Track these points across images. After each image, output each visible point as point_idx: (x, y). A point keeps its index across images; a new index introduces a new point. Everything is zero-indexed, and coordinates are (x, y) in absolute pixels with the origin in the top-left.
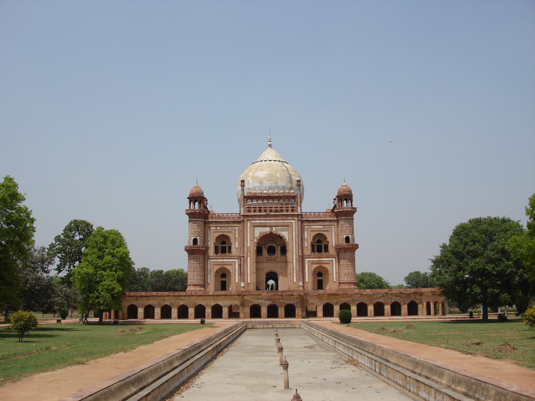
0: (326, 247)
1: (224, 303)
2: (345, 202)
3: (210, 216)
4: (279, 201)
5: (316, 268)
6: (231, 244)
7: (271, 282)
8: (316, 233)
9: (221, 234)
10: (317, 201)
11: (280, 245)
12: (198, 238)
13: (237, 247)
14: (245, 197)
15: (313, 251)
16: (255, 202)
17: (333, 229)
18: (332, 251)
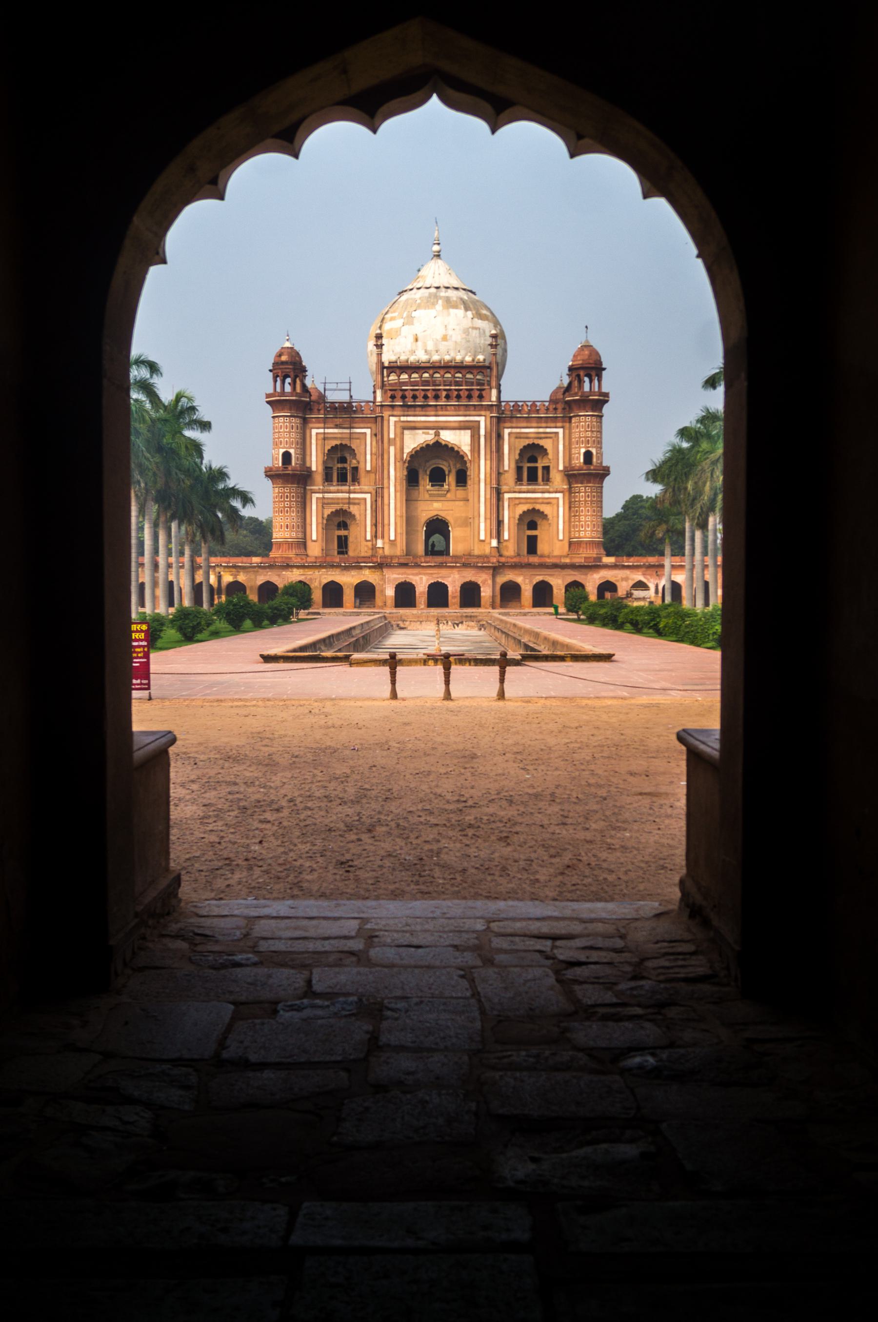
0: (547, 469)
1: (348, 580)
2: (586, 379)
5: (524, 512)
6: (358, 462)
7: (437, 538)
8: (527, 442)
9: (338, 442)
10: (531, 379)
11: (455, 465)
12: (292, 451)
13: (368, 468)
14: (383, 367)
15: (519, 479)
16: (404, 377)
17: (561, 436)
18: (557, 478)
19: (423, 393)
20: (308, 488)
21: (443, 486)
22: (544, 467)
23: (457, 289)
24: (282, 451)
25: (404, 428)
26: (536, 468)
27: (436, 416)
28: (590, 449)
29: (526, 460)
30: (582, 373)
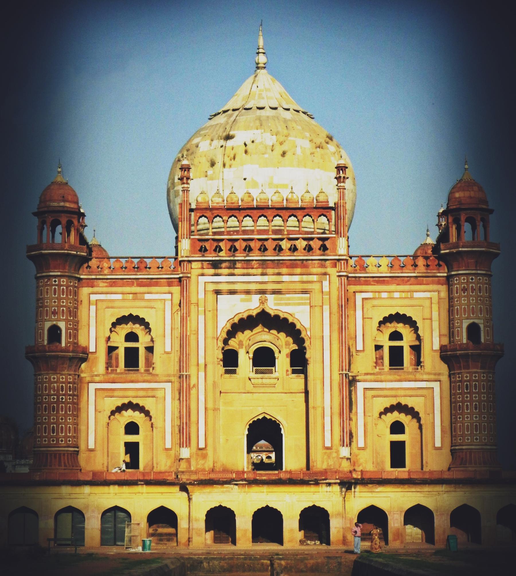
0: (417, 349)
3: (94, 263)
4: (285, 221)
12: (62, 325)
13: (168, 349)
14: (191, 210)
19: (244, 244)
20: (83, 375)
21: (271, 372)
22: (412, 347)
23: (288, 110)
24: (48, 325)
25: (218, 292)
26: (402, 347)
27: (263, 274)
28: (476, 321)
29: (387, 336)
30: (463, 217)
